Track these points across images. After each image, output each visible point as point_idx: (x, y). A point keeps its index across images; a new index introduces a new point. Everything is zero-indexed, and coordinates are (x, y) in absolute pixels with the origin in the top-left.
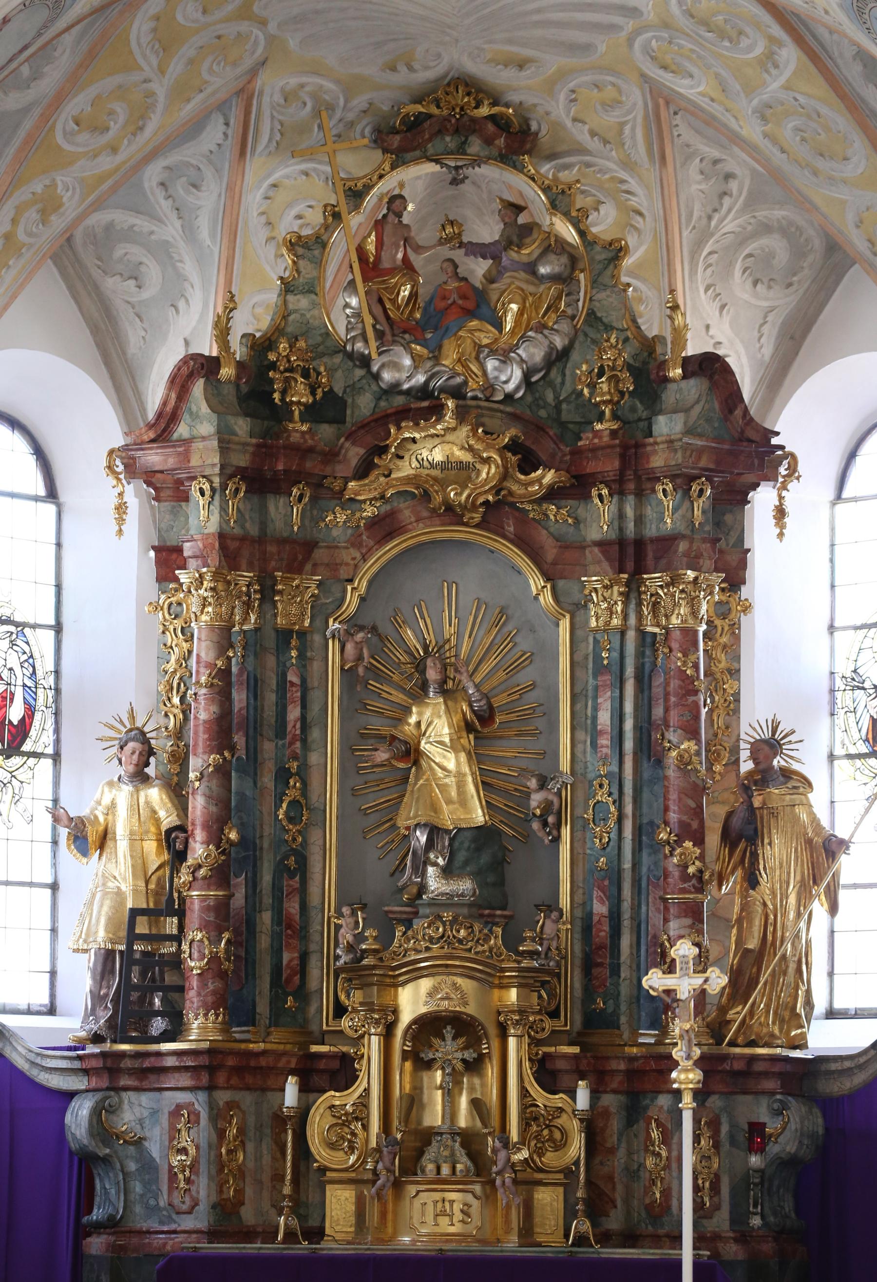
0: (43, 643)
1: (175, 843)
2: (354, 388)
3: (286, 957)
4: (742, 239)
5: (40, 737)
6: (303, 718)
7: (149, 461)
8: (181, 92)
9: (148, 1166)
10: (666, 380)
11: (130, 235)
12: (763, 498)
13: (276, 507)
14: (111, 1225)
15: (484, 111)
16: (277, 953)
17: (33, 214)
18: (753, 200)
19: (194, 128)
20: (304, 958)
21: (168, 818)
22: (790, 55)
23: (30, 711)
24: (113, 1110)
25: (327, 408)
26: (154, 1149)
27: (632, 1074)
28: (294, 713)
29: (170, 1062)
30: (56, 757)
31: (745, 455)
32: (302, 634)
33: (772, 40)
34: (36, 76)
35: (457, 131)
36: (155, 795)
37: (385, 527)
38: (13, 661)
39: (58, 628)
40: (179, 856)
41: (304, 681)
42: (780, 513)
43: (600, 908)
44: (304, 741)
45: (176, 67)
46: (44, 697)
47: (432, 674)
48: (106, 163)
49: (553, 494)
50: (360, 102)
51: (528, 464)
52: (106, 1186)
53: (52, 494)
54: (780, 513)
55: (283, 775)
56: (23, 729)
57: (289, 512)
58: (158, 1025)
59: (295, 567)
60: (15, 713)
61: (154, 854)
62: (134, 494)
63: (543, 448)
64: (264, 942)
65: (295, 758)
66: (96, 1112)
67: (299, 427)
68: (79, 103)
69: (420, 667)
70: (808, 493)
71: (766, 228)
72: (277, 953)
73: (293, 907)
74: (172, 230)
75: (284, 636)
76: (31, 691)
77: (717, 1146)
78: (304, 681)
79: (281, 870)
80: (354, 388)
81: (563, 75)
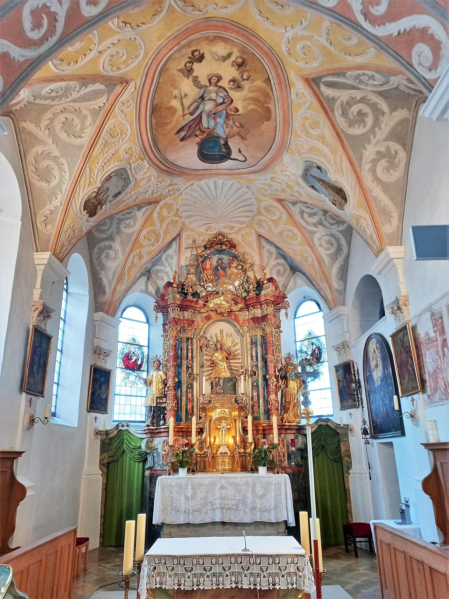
0: (145, 350)
1: (165, 383)
2: (202, 292)
3: (188, 407)
4: (274, 266)
5: (144, 367)
6: (192, 356)
7: (162, 307)
8: (166, 232)
9: (158, 454)
10: (263, 284)
11: (161, 271)
12: (283, 311)
13: (186, 313)
14: (150, 468)
15: (225, 240)
16: (187, 405)
17: (137, 258)
18: (277, 258)
19: (169, 245)
20: (193, 407)
21: (164, 377)
22: (285, 216)
23: (142, 362)
24: (152, 442)
25: (195, 294)
26: (159, 450)
27: (264, 430)
28: (190, 355)
29: (163, 430)
30: (148, 371)
31: (279, 301)
32: (192, 339)
33: (281, 213)
34: (134, 225)
35: (220, 244)
36: (161, 373)
37: (208, 318)
38: (139, 352)
39: (148, 347)
40: (166, 385)
41: (192, 348)
42: (286, 314)
43: (255, 394)
44: (192, 361)
45: (164, 227)
46: (145, 360)
47: (219, 346)
48: (152, 248)
49: (241, 310)
50: (201, 239)
51: (236, 303)
52: (150, 458)
53: (148, 322)
54: (286, 314)
55: (188, 367)
56: (141, 365)
57: (187, 314)
58: (162, 422)
59: (190, 325)
60: (139, 362)
61: (161, 386)
62: (160, 315)
63: (239, 300)
64: (184, 403)
65: (190, 364)
66: (147, 442)
67: (190, 297)
68: (144, 232)
69: (216, 345)
70: (291, 311)
71: (279, 264)
72: (187, 405)
73: (190, 396)
74: (168, 269)
75: (188, 339)
76: (142, 359)
77: (284, 446)
78: (192, 348)
79: (187, 387)
80: (202, 292)
81: (240, 230)
